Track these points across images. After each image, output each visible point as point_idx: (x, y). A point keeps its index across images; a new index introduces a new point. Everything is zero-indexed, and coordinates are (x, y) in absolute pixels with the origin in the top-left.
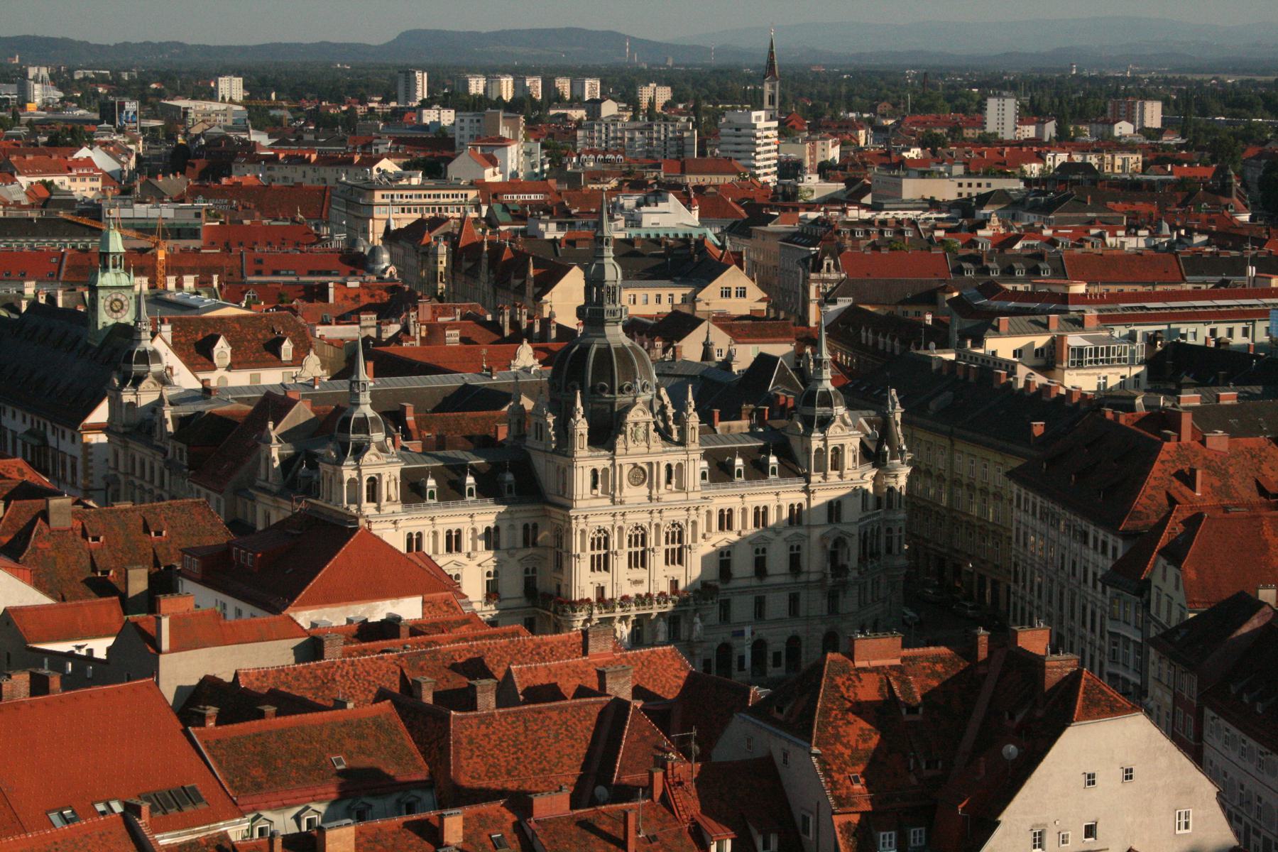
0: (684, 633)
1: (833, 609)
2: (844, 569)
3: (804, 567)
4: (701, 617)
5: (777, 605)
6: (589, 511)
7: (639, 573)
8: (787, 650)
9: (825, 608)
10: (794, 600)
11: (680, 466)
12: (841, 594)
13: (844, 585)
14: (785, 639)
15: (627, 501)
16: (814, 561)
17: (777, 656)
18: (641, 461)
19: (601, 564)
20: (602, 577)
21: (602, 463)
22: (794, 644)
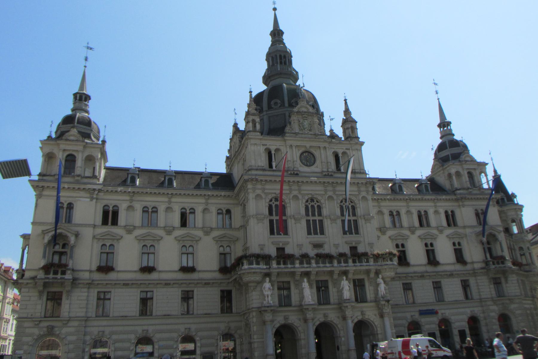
0: (370, 293)
1: (500, 294)
2: (502, 259)
3: (467, 257)
4: (383, 279)
5: (452, 289)
6: (253, 163)
7: (318, 238)
8: (471, 329)
9: (494, 292)
10: (465, 285)
11: (344, 153)
12: (503, 280)
13: (505, 272)
14: (466, 318)
15: (300, 174)
16: (474, 253)
17: (462, 334)
18: (308, 144)
19: (278, 227)
20: (281, 239)
21: (274, 143)
22: (473, 321)
